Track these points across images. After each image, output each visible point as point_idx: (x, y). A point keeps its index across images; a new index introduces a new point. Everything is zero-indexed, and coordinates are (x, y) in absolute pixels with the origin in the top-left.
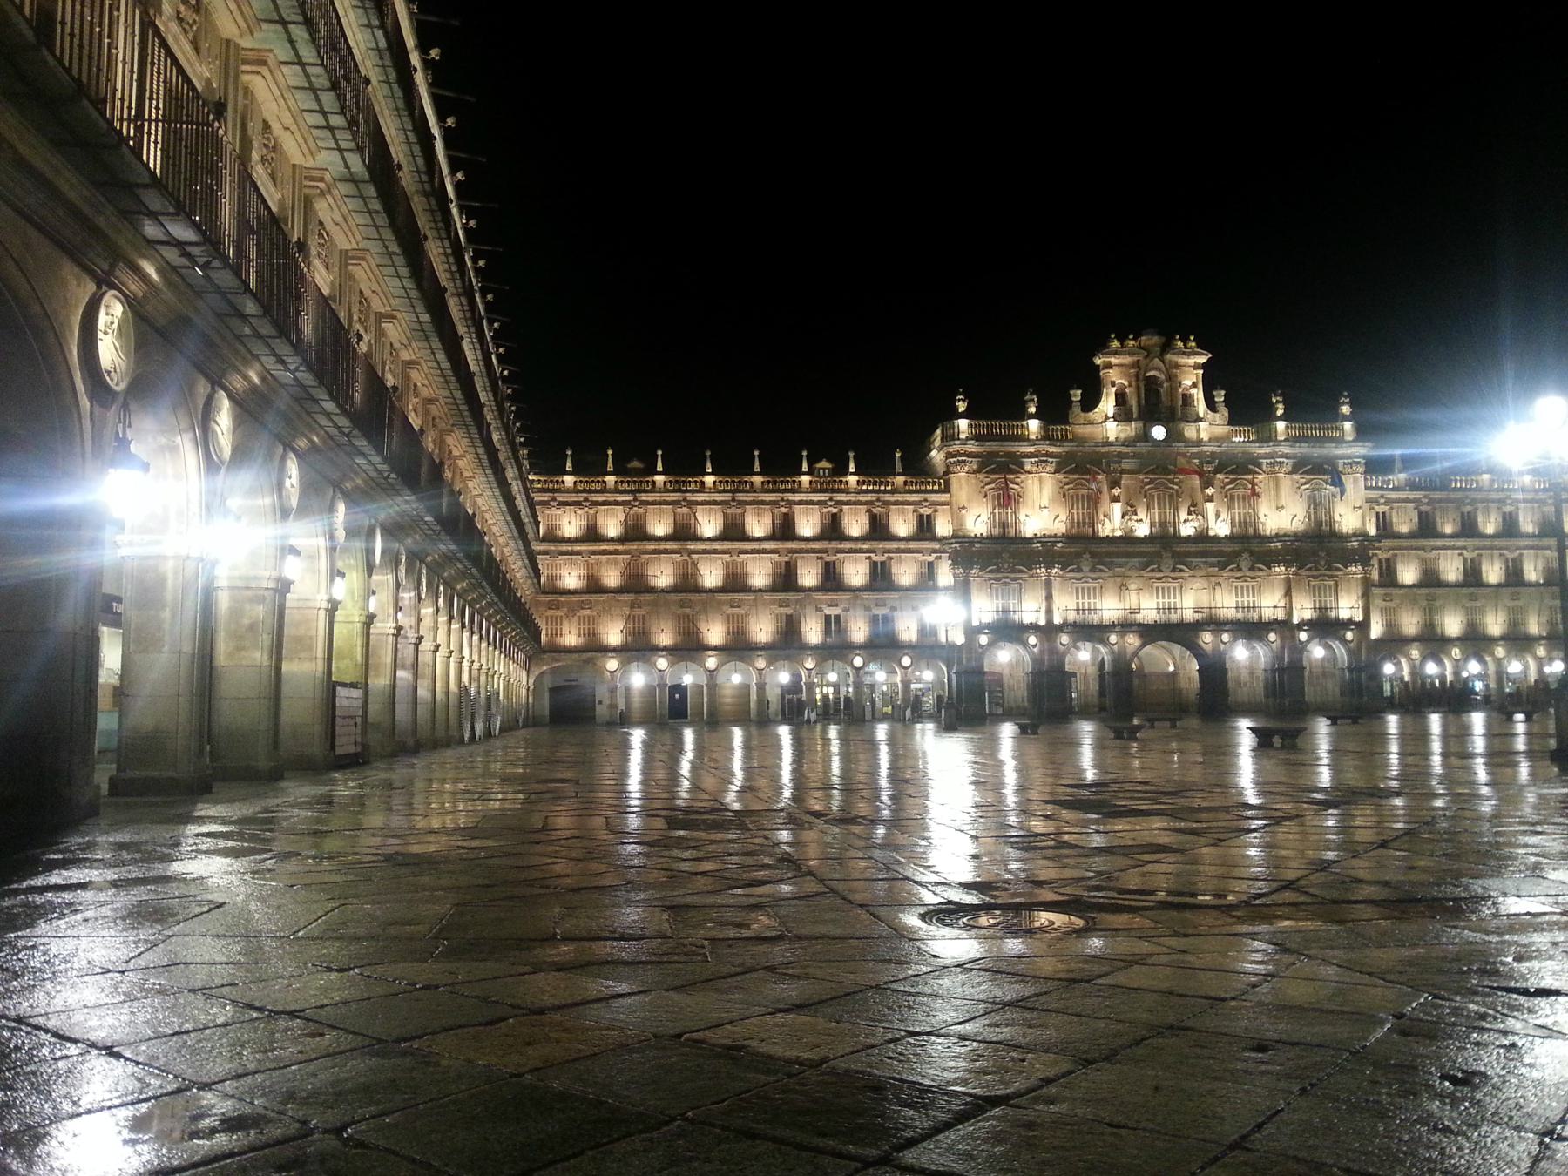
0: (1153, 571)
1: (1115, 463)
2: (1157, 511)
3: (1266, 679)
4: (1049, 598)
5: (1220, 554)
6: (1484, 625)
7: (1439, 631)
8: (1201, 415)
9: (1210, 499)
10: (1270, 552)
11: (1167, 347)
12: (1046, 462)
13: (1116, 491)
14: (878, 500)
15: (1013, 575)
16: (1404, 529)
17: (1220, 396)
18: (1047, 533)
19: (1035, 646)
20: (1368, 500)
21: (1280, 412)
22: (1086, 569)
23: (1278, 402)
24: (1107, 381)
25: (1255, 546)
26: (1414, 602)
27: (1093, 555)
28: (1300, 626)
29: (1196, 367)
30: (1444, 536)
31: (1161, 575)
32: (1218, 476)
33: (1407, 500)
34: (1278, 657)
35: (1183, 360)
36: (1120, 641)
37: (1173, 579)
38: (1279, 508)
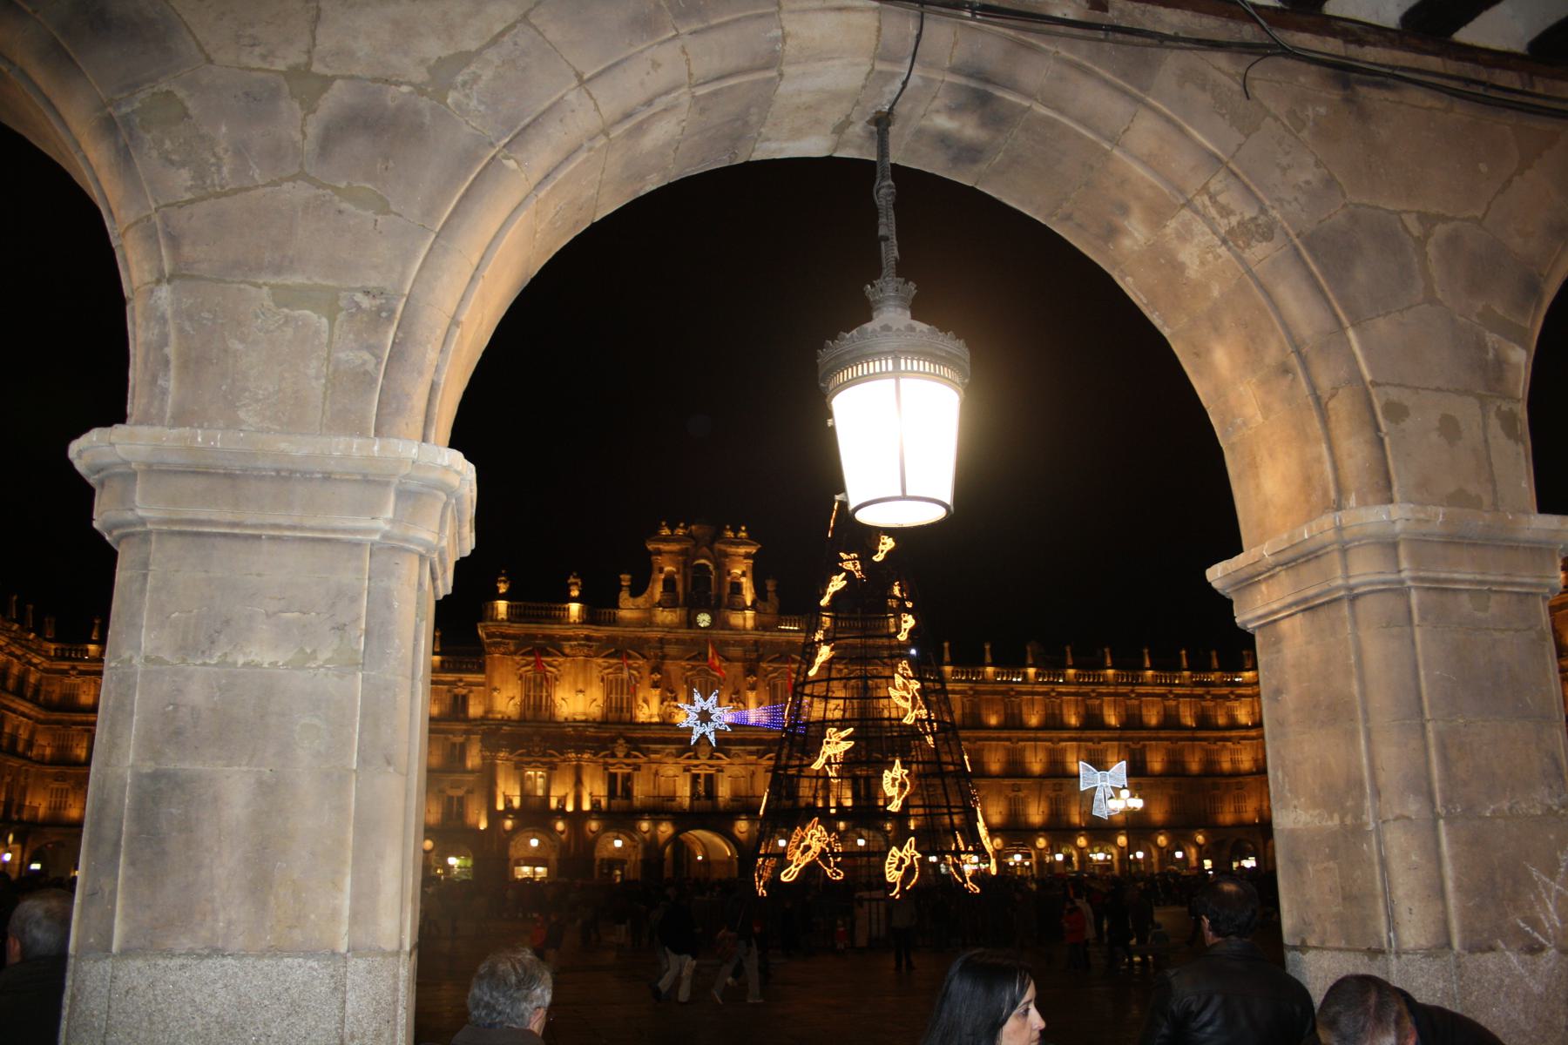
0: (689, 758)
4: (578, 782)
6: (1026, 815)
9: (753, 688)
11: (718, 536)
15: (544, 760)
17: (770, 585)
18: (578, 717)
19: (562, 832)
22: (620, 754)
24: (656, 567)
27: (628, 740)
29: (747, 556)
30: (989, 728)
32: (764, 665)
35: (733, 550)
36: (652, 829)
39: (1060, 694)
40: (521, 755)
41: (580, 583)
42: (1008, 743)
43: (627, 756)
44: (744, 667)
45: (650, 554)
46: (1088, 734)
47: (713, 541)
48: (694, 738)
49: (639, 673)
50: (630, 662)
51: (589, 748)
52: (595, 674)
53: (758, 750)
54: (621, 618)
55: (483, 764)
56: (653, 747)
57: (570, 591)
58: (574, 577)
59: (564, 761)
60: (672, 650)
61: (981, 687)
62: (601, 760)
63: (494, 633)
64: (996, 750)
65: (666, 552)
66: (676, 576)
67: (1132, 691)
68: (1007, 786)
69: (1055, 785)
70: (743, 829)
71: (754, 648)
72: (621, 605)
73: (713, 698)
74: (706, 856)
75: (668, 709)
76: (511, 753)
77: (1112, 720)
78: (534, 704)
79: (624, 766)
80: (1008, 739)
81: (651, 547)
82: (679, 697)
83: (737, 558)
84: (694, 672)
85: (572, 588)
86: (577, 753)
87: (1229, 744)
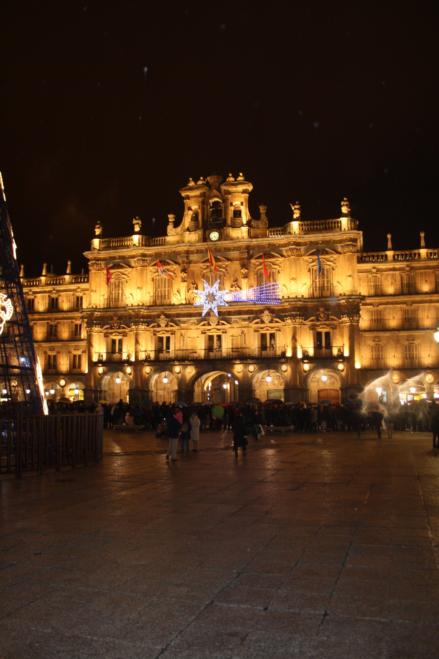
0: (204, 325)
1: (184, 257)
4: (137, 342)
7: (417, 361)
9: (246, 276)
10: (284, 310)
14: (54, 290)
16: (390, 290)
17: (262, 209)
19: (130, 374)
20: (360, 271)
22: (163, 325)
23: (295, 209)
24: (186, 207)
26: (397, 341)
27: (167, 316)
29: (244, 192)
31: (209, 327)
32: (253, 261)
33: (394, 269)
40: (107, 329)
41: (140, 223)
43: (167, 326)
44: (240, 264)
45: (183, 198)
47: (221, 184)
48: (204, 312)
49: (174, 274)
51: (143, 322)
52: (149, 277)
53: (249, 318)
54: (168, 242)
55: (87, 335)
56: (182, 319)
57: (134, 228)
58: (136, 219)
59: (131, 331)
60: (193, 257)
62: (152, 329)
63: (91, 258)
64: (429, 310)
71: (246, 251)
72: (168, 234)
73: (216, 285)
75: (192, 294)
76: (102, 327)
78: (115, 298)
79: (166, 333)
81: (183, 195)
85: (136, 226)
86: (136, 325)
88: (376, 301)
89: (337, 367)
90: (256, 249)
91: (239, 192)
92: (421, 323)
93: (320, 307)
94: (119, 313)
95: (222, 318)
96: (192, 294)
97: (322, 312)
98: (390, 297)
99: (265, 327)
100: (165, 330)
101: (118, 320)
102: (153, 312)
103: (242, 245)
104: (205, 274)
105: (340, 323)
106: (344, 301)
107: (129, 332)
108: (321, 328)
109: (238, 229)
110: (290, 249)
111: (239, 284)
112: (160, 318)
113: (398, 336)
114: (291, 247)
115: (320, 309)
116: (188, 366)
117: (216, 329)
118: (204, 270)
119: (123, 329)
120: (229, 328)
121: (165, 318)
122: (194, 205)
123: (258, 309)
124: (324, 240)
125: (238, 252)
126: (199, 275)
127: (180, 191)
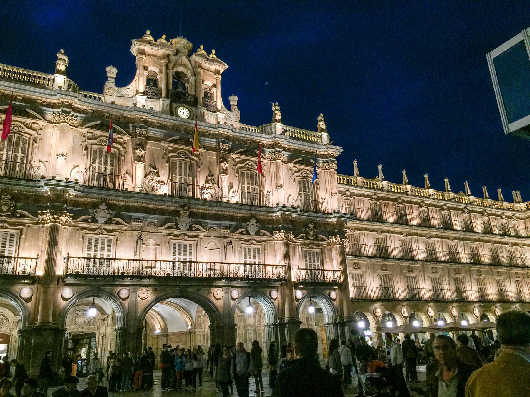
0: (170, 227)
1: (141, 127)
2: (178, 176)
3: (269, 334)
4: (53, 243)
5: (231, 218)
8: (219, 108)
9: (225, 172)
10: (271, 221)
12: (69, 113)
13: (140, 152)
15: (13, 220)
16: (364, 215)
17: (234, 100)
19: (28, 300)
21: (278, 117)
22: (102, 220)
25: (261, 215)
27: (110, 207)
28: (296, 285)
29: (217, 72)
31: (176, 232)
32: (233, 156)
33: (363, 195)
34: (279, 313)
35: (206, 65)
37: (190, 237)
38: (279, 186)
39: (427, 205)
41: (67, 60)
42: (401, 236)
44: (217, 156)
46: (448, 233)
49: (124, 148)
50: (115, 136)
56: (134, 214)
59: (38, 223)
61: (381, 194)
65: (150, 55)
66: (158, 77)
67: (465, 207)
68: (405, 266)
69: (432, 268)
70: (219, 296)
72: (106, 91)
74: (165, 329)
77: (458, 226)
79: (105, 232)
80: (401, 233)
82: (162, 173)
83: (209, 73)
84: (176, 154)
85: (58, 62)
87: (519, 248)
88: (353, 225)
89: (329, 295)
90: (236, 142)
91: (210, 71)
92: (390, 253)
93: (310, 223)
94: (18, 189)
95: (195, 221)
96: (151, 182)
97: (311, 230)
98: (365, 223)
99: (250, 240)
100: (104, 229)
101: (11, 200)
102: (85, 197)
103: (222, 132)
104: (171, 159)
105: (327, 244)
106: (335, 220)
107: (32, 224)
108: (309, 248)
109: (212, 113)
110: (277, 151)
111: (216, 180)
112: (98, 208)
113: (374, 265)
114: (278, 149)
115: (310, 225)
116: (141, 288)
117: (187, 235)
118: (169, 153)
119: (20, 217)
120: (204, 236)
121: (106, 209)
122: (153, 66)
123: (241, 215)
124: (307, 150)
125: (215, 140)
126: (161, 158)
127: (134, 41)
